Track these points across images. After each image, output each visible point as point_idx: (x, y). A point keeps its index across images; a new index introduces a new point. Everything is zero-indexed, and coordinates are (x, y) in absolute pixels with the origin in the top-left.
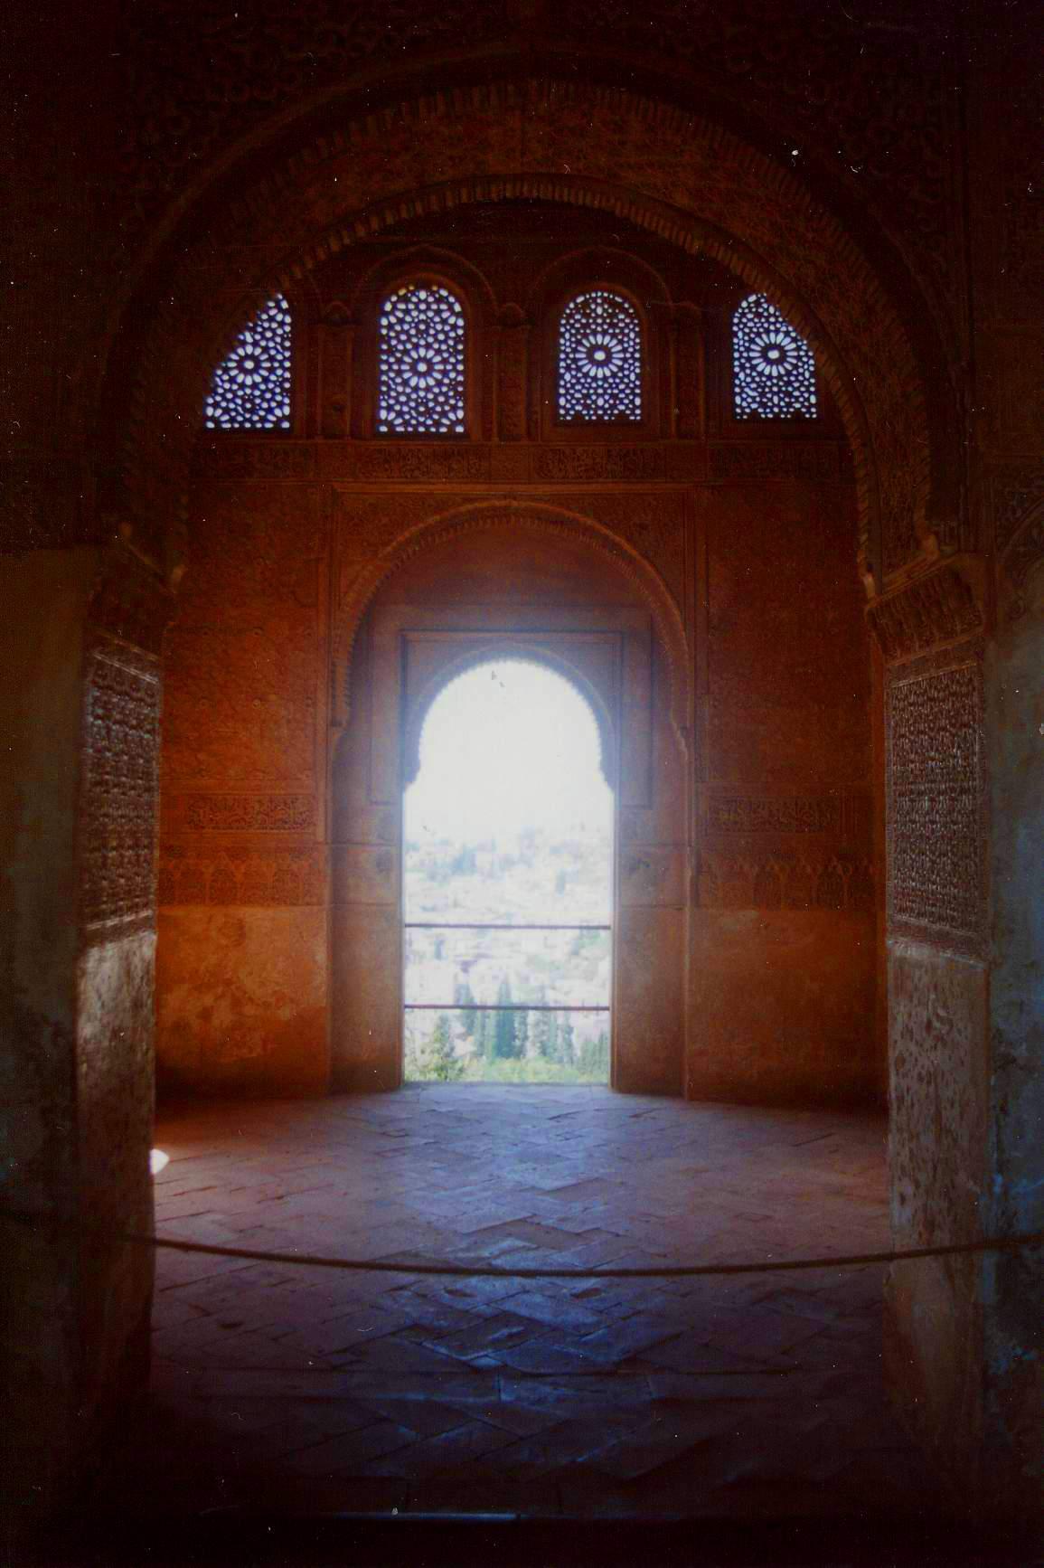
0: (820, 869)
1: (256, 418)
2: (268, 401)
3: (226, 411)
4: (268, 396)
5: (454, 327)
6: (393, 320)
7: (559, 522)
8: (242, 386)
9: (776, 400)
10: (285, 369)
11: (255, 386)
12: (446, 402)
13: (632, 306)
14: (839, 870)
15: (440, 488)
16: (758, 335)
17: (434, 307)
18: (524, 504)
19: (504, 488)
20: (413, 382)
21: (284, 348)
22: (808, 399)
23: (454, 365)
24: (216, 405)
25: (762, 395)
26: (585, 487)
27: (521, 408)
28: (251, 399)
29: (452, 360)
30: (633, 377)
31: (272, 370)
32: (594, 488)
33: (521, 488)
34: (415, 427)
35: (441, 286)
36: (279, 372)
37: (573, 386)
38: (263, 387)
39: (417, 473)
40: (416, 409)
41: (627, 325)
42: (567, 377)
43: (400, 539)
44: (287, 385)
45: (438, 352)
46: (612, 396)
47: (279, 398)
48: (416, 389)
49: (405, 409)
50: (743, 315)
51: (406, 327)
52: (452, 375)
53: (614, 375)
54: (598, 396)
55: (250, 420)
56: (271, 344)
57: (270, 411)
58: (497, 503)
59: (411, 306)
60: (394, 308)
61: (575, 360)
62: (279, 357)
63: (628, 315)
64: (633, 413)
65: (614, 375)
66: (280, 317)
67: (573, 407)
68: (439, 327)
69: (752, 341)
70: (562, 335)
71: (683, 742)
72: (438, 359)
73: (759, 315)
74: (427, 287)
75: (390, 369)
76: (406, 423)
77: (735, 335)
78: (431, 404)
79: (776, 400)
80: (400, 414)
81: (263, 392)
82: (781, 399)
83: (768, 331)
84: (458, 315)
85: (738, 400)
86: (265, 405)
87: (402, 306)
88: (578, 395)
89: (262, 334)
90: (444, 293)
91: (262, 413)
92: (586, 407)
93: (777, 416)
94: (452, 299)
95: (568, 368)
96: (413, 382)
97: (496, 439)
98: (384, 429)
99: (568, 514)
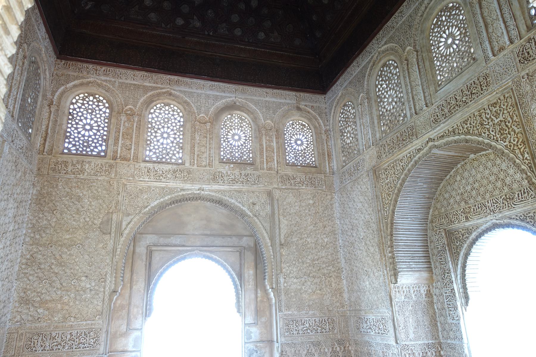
0: (331, 350)
1: (88, 150)
2: (95, 143)
3: (74, 145)
4: (95, 141)
5: (179, 121)
6: (154, 116)
7: (220, 202)
8: (84, 136)
9: (301, 158)
10: (104, 131)
11: (90, 136)
12: (175, 150)
13: (248, 120)
14: (338, 349)
15: (172, 184)
16: (294, 135)
17: (171, 113)
18: (206, 193)
19: (197, 187)
20: (161, 141)
21: (106, 123)
22: (312, 159)
23: (179, 136)
24: (69, 143)
25: (296, 156)
26: (231, 187)
27: (206, 155)
28: (88, 141)
29: (178, 134)
30: (249, 146)
31: (98, 131)
32: (236, 187)
33: (204, 186)
34: (161, 159)
35: (174, 106)
36: (102, 132)
37: (226, 148)
38: (93, 137)
39: (161, 177)
40: (162, 152)
41: (247, 127)
42: (224, 144)
43: (152, 205)
44: (105, 137)
45: (172, 130)
46: (241, 153)
47: (100, 142)
48: (162, 144)
49: (157, 151)
50: (288, 128)
51: (159, 119)
52: (178, 140)
53: (242, 145)
54: (236, 152)
55: (86, 151)
56: (99, 120)
57: (96, 147)
58: (195, 192)
59: (162, 112)
60: (155, 111)
61: (227, 139)
62: (102, 126)
63: (247, 124)
64: (249, 160)
65: (242, 145)
66: (104, 110)
67: (226, 156)
68: (173, 121)
69: (291, 137)
70: (222, 129)
71: (272, 295)
72: (172, 133)
73: (293, 128)
74: (169, 105)
75: (152, 135)
76: (157, 157)
77: (285, 134)
78: (168, 150)
79: (301, 158)
80: (155, 153)
81: (93, 139)
82: (303, 159)
83: (297, 134)
84: (181, 117)
85: (287, 158)
86: (93, 145)
87: (158, 111)
88: (228, 152)
89: (95, 115)
90: (176, 108)
91: (92, 148)
92: (231, 156)
93: (301, 164)
94: (179, 111)
95: (224, 141)
96: (161, 141)
97: (195, 167)
98: (147, 159)
99: (224, 197)
